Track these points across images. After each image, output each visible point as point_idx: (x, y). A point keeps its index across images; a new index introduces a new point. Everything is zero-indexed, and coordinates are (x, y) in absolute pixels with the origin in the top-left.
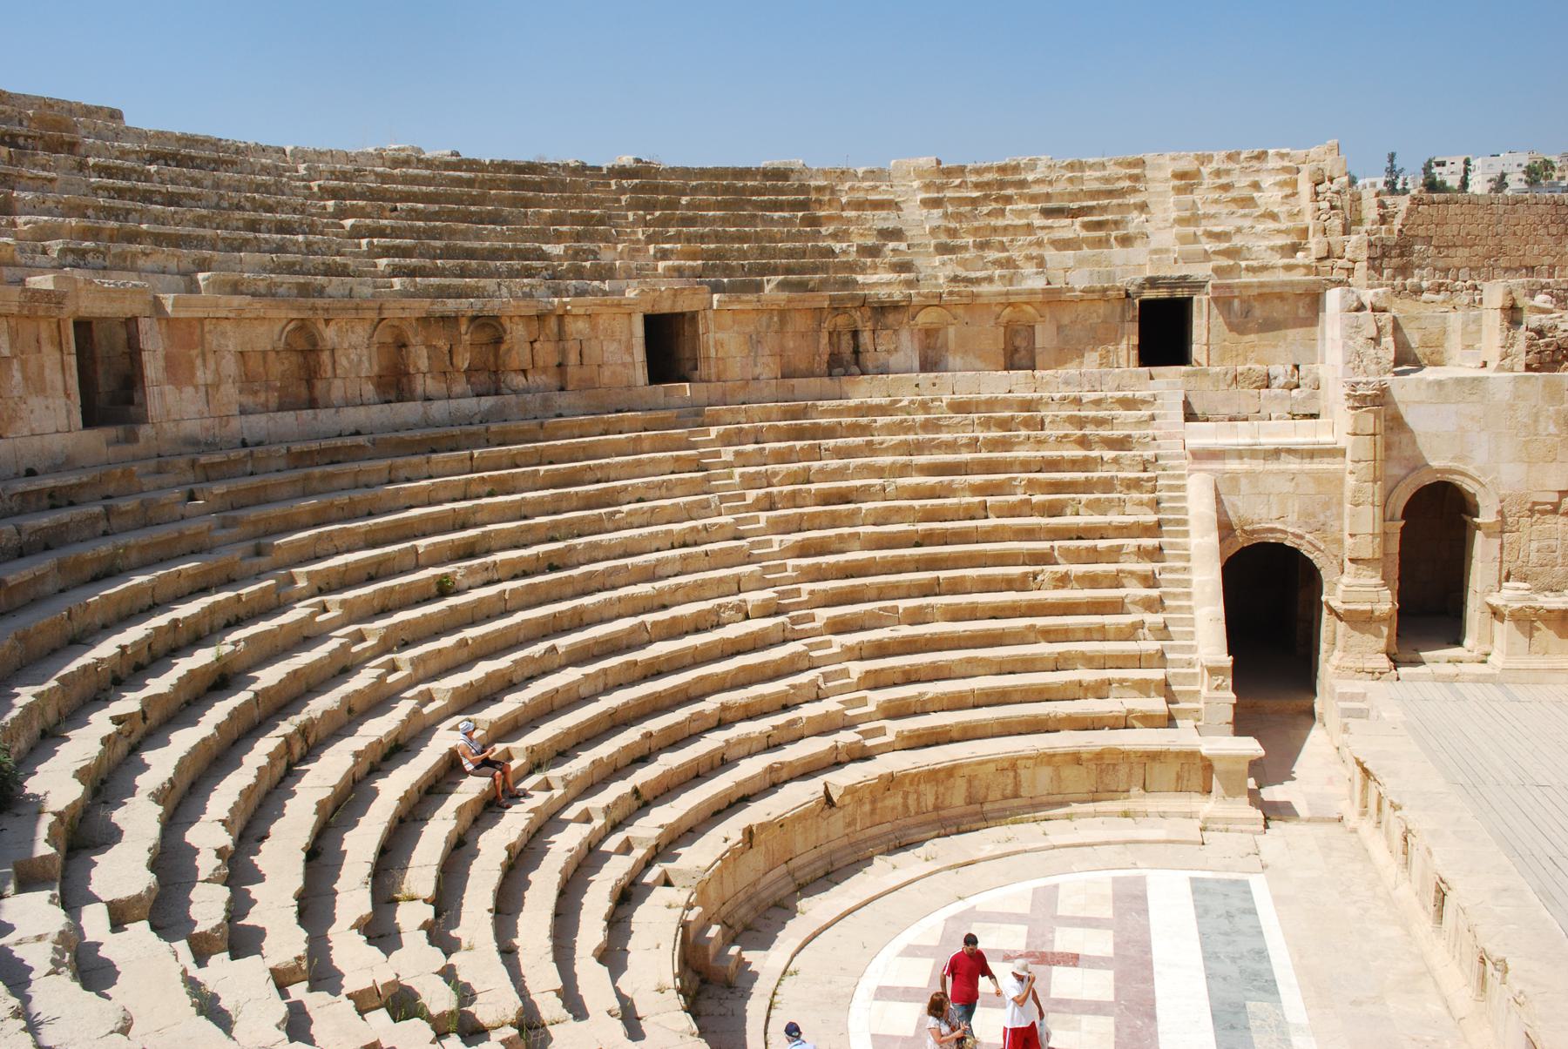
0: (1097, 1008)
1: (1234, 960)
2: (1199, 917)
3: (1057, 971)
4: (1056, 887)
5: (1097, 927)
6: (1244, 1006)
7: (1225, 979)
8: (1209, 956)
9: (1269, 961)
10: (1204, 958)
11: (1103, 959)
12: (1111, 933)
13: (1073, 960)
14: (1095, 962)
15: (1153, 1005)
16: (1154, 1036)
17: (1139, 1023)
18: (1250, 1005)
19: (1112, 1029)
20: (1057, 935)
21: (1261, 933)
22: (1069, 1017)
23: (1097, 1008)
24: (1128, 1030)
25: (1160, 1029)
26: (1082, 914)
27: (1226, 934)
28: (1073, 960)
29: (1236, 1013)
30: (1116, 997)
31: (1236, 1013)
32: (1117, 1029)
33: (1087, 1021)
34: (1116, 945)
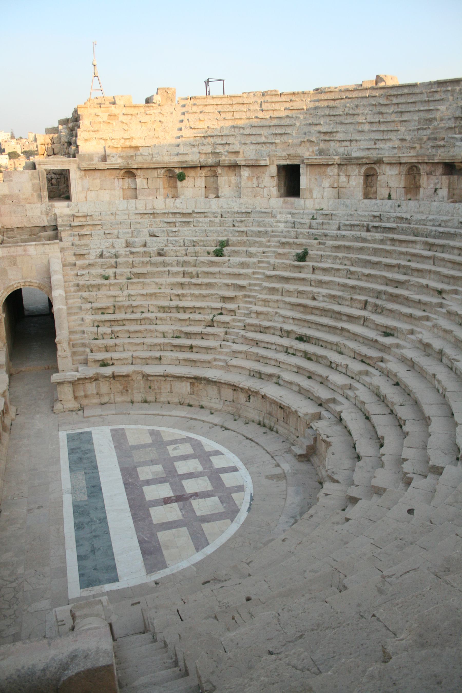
0: (148, 482)
1: (92, 521)
2: (110, 547)
3: (171, 494)
4: (197, 550)
5: (163, 524)
6: (88, 497)
7: (96, 508)
8: (104, 520)
9: (75, 524)
10: (106, 518)
11: (154, 506)
12: (155, 522)
13: (167, 501)
14: (156, 503)
15: (126, 488)
16: (123, 476)
17: (130, 480)
18: (86, 498)
19: (140, 476)
20: (180, 514)
21: (77, 541)
22: (158, 477)
23: (148, 482)
24: (133, 476)
25: (122, 480)
26: (174, 531)
27: (95, 537)
28: (167, 501)
29: (92, 493)
30: (142, 489)
31: (92, 493)
32: (138, 476)
33: (151, 477)
34: (149, 515)
